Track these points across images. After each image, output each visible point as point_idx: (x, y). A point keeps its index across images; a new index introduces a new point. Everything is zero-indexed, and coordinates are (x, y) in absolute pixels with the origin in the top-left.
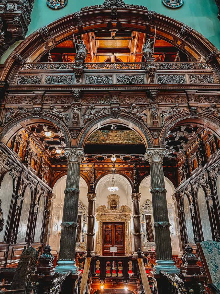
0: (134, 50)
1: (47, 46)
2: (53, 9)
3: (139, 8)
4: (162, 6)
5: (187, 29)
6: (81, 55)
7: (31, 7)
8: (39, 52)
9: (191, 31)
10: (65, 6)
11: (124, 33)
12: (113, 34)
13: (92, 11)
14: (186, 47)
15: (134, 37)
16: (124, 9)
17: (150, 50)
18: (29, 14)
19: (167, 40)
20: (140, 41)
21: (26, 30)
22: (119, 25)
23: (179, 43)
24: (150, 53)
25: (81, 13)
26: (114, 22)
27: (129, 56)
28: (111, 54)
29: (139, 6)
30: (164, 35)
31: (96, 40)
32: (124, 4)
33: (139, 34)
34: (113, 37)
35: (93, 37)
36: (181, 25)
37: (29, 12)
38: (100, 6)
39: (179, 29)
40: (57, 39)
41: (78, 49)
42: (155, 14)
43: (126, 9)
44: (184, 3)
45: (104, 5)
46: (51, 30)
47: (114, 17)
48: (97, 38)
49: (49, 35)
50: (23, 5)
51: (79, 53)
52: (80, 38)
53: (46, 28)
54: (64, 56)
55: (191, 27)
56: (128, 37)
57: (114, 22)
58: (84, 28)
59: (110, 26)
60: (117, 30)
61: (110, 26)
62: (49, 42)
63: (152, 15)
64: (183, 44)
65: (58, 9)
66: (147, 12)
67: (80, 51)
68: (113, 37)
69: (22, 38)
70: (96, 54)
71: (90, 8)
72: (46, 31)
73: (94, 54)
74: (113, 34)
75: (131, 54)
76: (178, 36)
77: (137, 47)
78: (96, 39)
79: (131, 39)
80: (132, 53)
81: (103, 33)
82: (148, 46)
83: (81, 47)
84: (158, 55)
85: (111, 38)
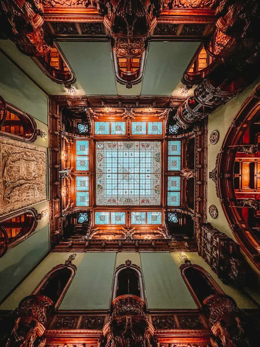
0: (253, 159)
1: (246, 229)
2: (217, 215)
3: (218, 159)
4: (215, 145)
5: (233, 123)
6: (253, 205)
7: (216, 229)
8: (251, 237)
9: (235, 119)
10: (216, 207)
11: (237, 168)
12: (236, 176)
13: (219, 191)
14: (249, 119)
15: (240, 160)
16: (218, 169)
17: (251, 148)
18: (221, 233)
19: (242, 136)
20: (243, 155)
21: (231, 240)
22: (230, 172)
23: (245, 126)
24: (254, 148)
25: (220, 198)
26: (227, 175)
27: (258, 163)
28: (255, 178)
29: (216, 159)
30: (238, 139)
31: (243, 188)
32: (215, 169)
33: (237, 157)
34: (240, 175)
35: (240, 191)
36: (230, 128)
37: (219, 232)
38: (216, 185)
39: (233, 128)
40: (240, 219)
41: (249, 206)
42: (222, 148)
43: (219, 167)
44: (216, 129)
45: (215, 182)
46: (232, 223)
47: (223, 176)
48: (240, 188)
49: (236, 225)
50: (214, 235)
51: (252, 206)
52: (239, 200)
53: (230, 225)
54: (257, 216)
55: (232, 120)
56: (240, 164)
57: (227, 175)
58: (231, 197)
59: (230, 179)
60: (234, 173)
61: (230, 179)
62: (242, 226)
63: (222, 150)
64: (246, 122)
65: (217, 212)
66: (221, 153)
67: (250, 204)
68: (240, 175)
69: (238, 246)
70: (256, 190)
71: (217, 191)
72: (232, 226)
73: (255, 191)
74: (236, 176)
75: (256, 161)
76: (239, 128)
77: (250, 157)
78: (242, 189)
79: (242, 162)
80: (256, 160)
81: (237, 183)
82: (246, 150)
83: (247, 203)
84: (258, 139)
85: (240, 177)
